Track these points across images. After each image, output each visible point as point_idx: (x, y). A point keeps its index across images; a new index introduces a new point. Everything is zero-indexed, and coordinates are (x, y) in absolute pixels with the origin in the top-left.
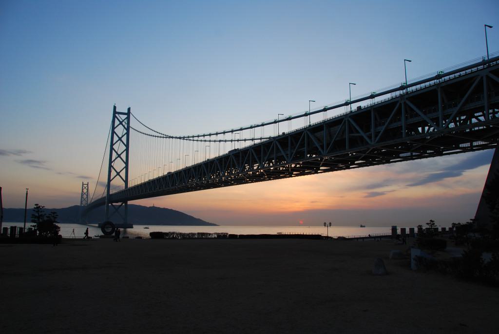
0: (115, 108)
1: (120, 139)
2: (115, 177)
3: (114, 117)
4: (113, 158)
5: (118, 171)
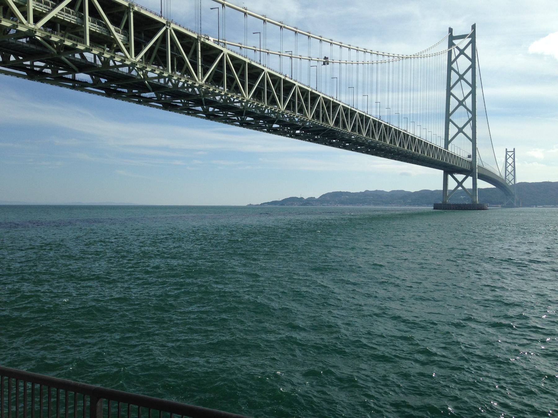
0: (451, 30)
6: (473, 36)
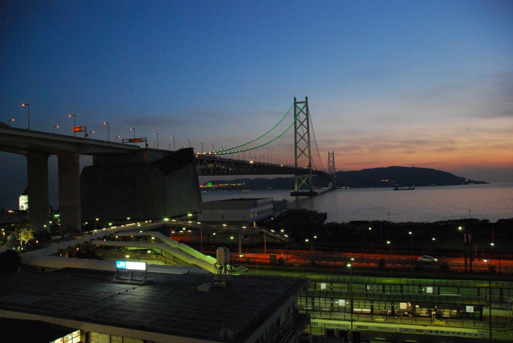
0: (295, 99)
1: (302, 124)
2: (301, 154)
3: (295, 106)
4: (298, 140)
5: (303, 150)
6: (306, 103)
